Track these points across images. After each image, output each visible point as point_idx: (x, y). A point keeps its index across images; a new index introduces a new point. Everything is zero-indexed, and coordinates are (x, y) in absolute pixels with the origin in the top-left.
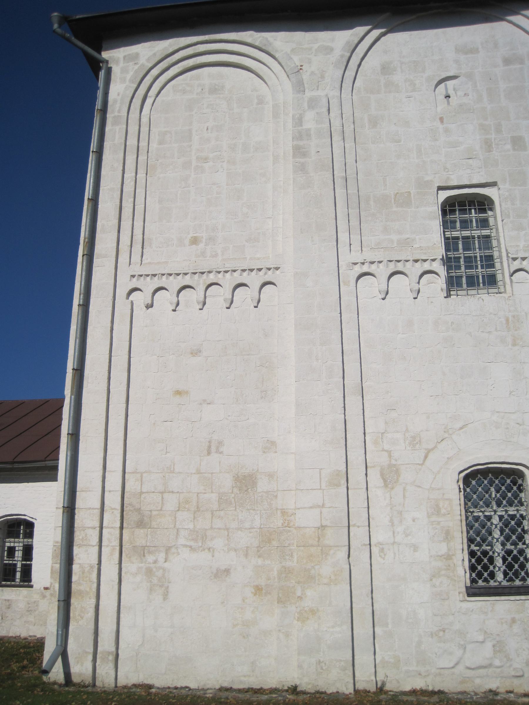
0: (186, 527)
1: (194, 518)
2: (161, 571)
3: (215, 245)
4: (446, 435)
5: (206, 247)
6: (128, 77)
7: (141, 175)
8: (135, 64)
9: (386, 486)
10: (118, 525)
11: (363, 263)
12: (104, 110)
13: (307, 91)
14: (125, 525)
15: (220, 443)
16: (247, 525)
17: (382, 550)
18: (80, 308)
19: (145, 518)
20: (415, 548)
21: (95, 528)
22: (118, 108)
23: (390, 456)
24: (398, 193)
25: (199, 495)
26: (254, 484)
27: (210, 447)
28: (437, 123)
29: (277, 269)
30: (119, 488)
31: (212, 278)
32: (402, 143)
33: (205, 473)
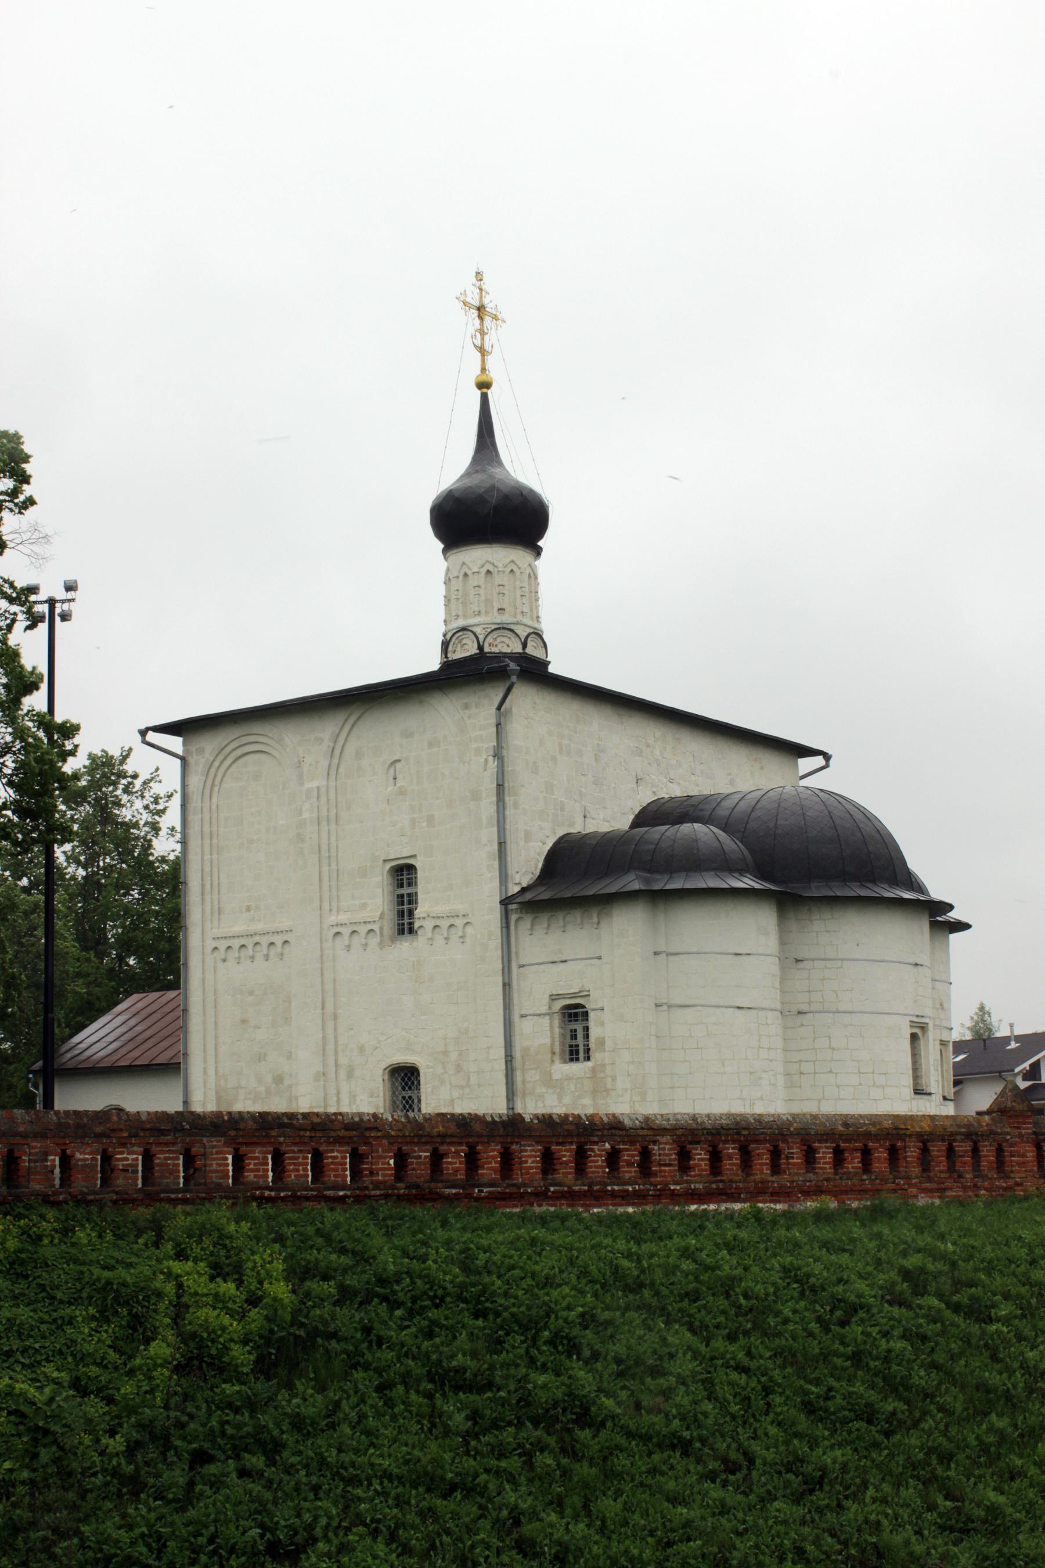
15: (265, 1055)
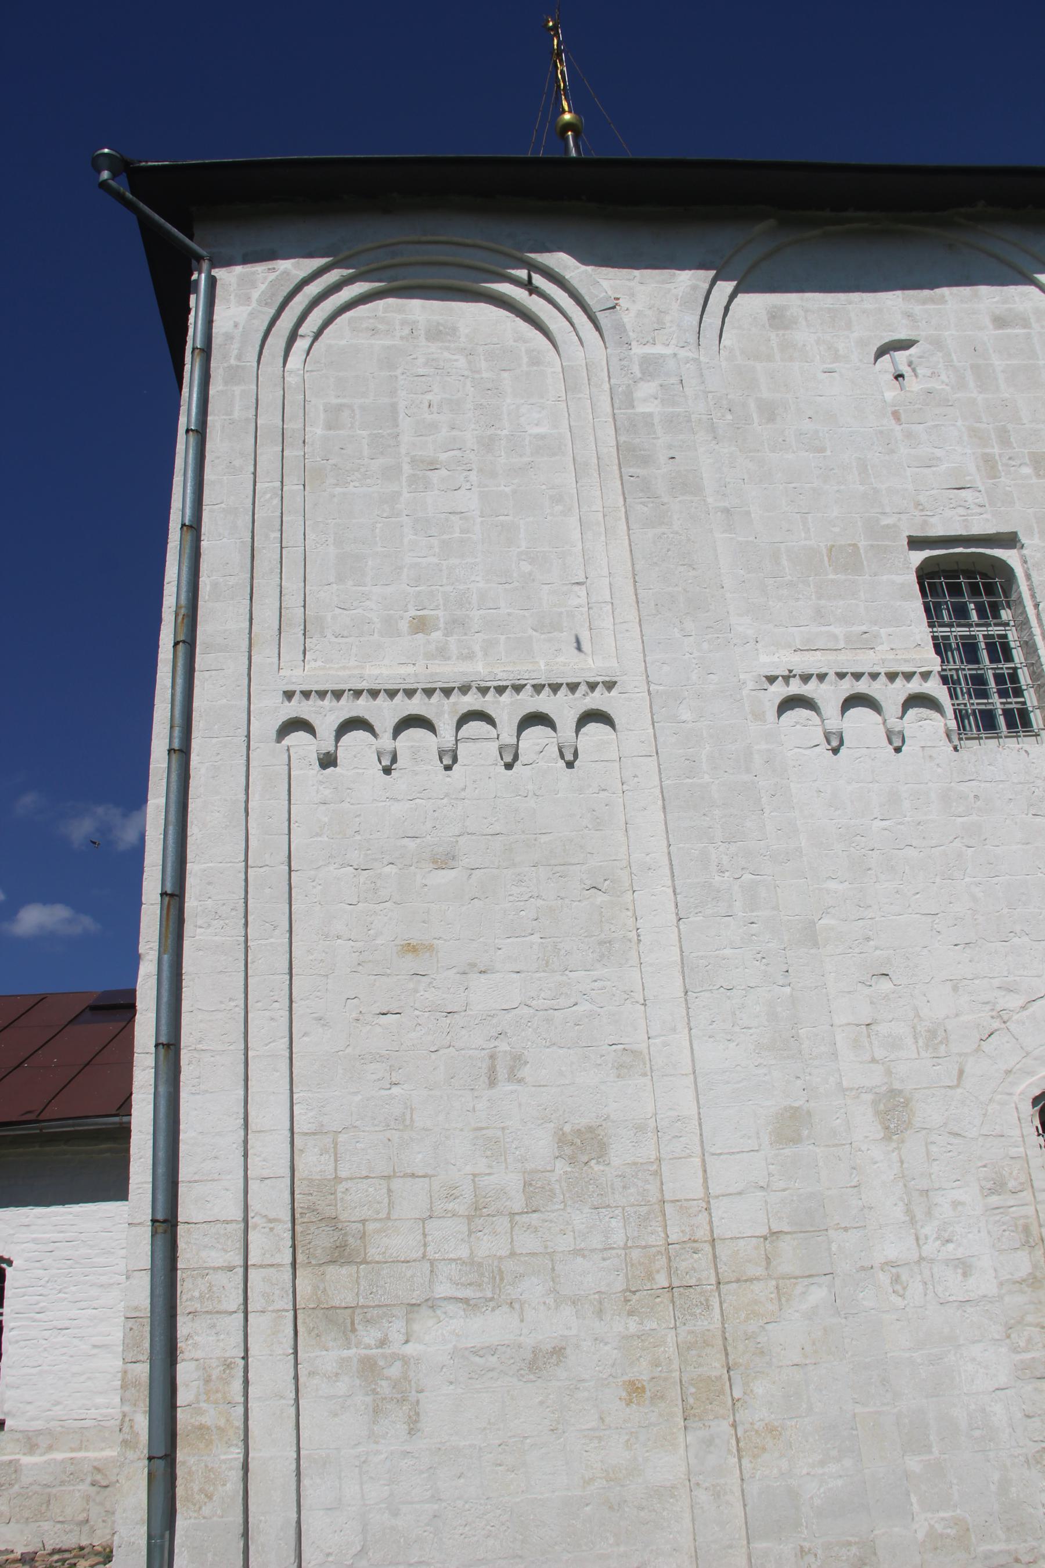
0: (451, 1256)
1: (470, 1233)
2: (398, 1364)
3: (466, 634)
4: (996, 1024)
5: (448, 639)
6: (255, 295)
7: (292, 486)
8: (269, 269)
9: (888, 1138)
10: (288, 1259)
11: (787, 679)
12: (206, 352)
13: (634, 343)
14: (300, 1258)
15: (518, 1060)
16: (596, 1241)
17: (896, 1279)
18: (174, 757)
19: (351, 1240)
20: (965, 1267)
21: (231, 1269)
22: (236, 352)
23: (889, 1072)
24: (833, 546)
25: (476, 1179)
26: (601, 1150)
27: (492, 1069)
28: (889, 423)
29: (610, 685)
30: (287, 1172)
31: (471, 701)
32: (828, 453)
33: (487, 1128)
